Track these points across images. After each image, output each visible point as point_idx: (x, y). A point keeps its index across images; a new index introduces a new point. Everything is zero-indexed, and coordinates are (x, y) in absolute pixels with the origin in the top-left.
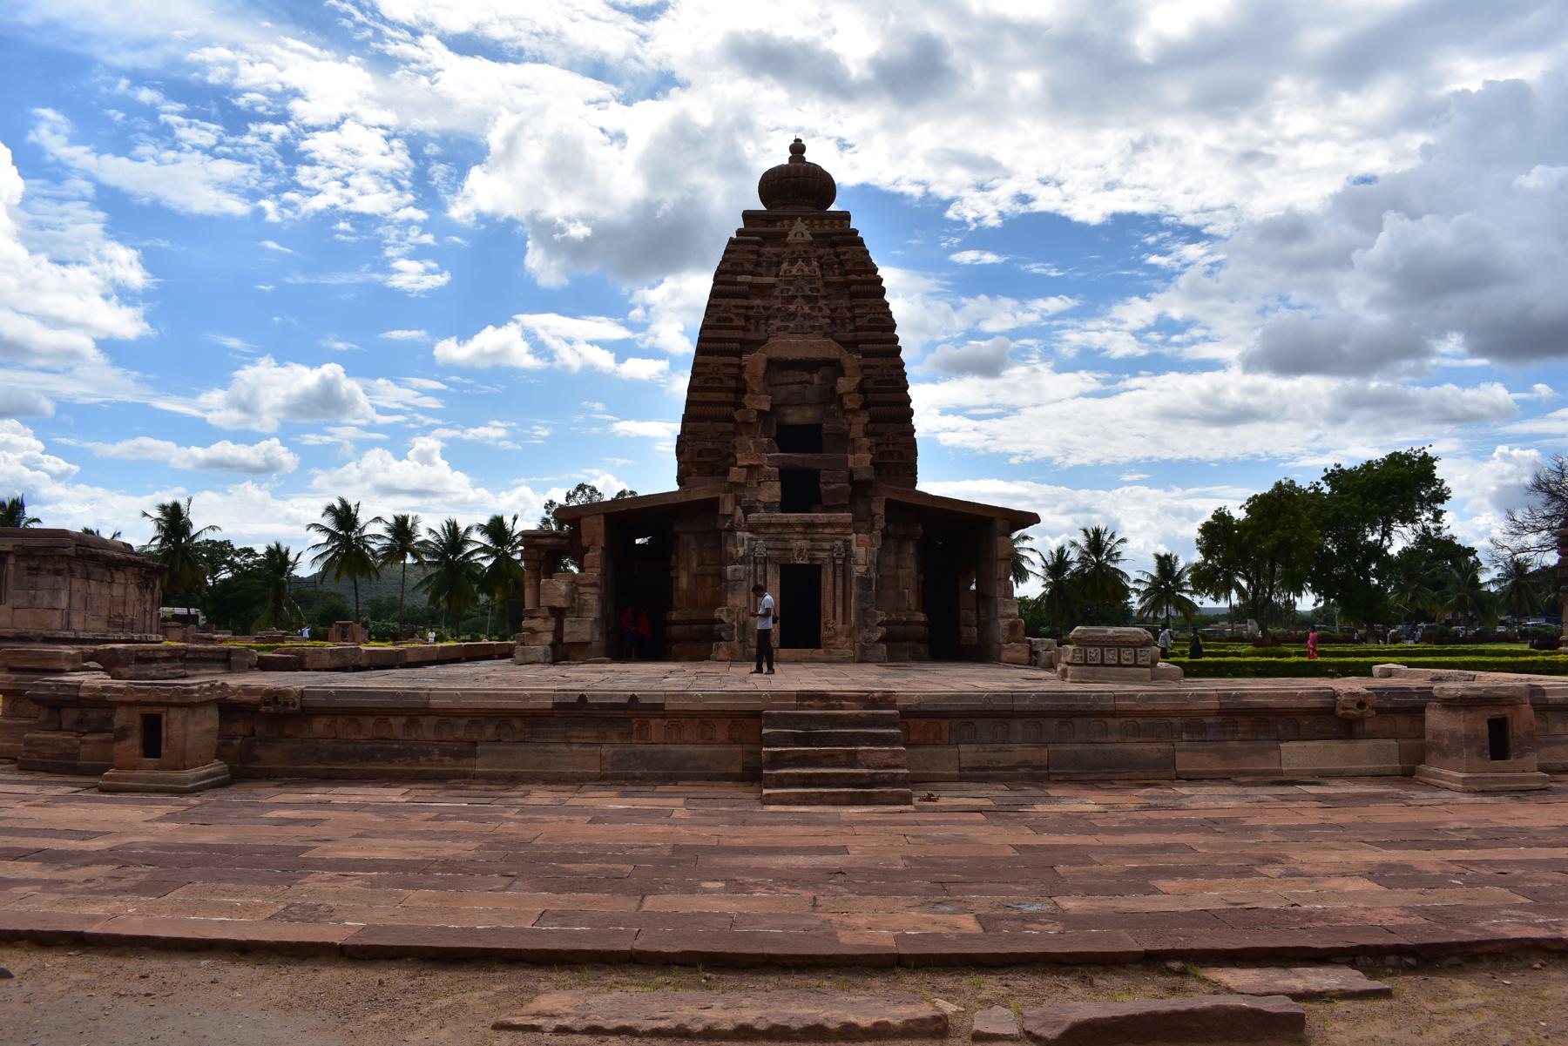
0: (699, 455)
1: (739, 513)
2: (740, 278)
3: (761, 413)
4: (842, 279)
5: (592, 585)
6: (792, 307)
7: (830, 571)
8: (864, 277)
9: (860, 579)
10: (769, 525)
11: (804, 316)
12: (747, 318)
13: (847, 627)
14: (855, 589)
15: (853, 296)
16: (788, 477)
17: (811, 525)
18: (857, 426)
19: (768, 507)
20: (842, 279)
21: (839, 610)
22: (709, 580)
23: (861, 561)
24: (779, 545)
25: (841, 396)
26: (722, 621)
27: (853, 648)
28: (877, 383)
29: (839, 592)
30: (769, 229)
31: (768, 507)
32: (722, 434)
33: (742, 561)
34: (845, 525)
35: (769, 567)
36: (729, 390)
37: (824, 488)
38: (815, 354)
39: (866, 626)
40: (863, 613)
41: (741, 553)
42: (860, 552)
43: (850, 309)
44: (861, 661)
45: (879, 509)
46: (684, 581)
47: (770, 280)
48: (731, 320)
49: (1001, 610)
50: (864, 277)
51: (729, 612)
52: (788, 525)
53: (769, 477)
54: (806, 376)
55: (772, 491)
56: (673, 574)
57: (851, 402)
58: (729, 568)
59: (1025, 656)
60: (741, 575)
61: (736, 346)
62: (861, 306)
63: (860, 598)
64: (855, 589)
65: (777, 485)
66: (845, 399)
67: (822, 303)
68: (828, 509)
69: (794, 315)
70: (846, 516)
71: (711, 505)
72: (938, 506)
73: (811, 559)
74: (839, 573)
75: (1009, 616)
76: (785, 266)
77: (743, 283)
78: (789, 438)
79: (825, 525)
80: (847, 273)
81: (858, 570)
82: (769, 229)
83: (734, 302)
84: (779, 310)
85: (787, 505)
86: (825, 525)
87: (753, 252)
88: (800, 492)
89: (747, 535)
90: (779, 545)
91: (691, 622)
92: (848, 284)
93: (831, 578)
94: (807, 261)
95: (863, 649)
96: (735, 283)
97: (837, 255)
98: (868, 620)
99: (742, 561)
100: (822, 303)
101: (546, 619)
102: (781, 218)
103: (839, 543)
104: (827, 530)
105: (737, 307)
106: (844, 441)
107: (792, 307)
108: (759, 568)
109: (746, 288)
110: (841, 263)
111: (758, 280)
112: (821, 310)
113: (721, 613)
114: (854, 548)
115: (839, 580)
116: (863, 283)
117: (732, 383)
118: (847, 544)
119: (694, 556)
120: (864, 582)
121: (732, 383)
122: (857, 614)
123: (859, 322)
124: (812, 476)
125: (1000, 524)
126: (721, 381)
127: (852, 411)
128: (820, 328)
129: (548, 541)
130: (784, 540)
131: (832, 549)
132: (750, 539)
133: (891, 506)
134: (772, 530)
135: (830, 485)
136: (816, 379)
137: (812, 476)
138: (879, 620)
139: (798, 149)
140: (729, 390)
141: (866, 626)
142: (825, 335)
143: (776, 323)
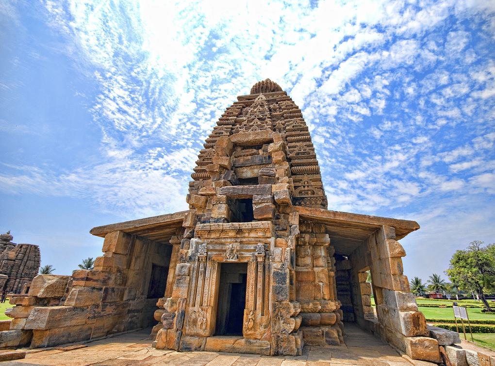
3: (222, 167)
4: (280, 113)
9: (276, 274)
10: (210, 232)
11: (258, 126)
13: (265, 318)
16: (229, 201)
17: (240, 231)
18: (280, 170)
23: (277, 259)
24: (218, 247)
28: (298, 154)
29: (260, 286)
31: (217, 220)
34: (265, 230)
35: (209, 265)
37: (255, 207)
41: (190, 254)
42: (276, 252)
43: (283, 125)
45: (294, 221)
53: (219, 201)
54: (255, 151)
55: (221, 211)
57: (278, 157)
63: (278, 291)
66: (273, 155)
74: (260, 269)
79: (250, 230)
81: (275, 266)
84: (245, 125)
85: (227, 220)
86: (250, 230)
88: (241, 210)
90: (218, 247)
93: (254, 275)
98: (284, 312)
103: (260, 244)
104: (253, 235)
106: (272, 179)
107: (251, 124)
112: (267, 123)
114: (272, 248)
115: (260, 274)
120: (280, 277)
122: (274, 306)
123: (287, 128)
131: (254, 250)
133: (303, 220)
134: (213, 236)
137: (248, 202)
138: (293, 311)
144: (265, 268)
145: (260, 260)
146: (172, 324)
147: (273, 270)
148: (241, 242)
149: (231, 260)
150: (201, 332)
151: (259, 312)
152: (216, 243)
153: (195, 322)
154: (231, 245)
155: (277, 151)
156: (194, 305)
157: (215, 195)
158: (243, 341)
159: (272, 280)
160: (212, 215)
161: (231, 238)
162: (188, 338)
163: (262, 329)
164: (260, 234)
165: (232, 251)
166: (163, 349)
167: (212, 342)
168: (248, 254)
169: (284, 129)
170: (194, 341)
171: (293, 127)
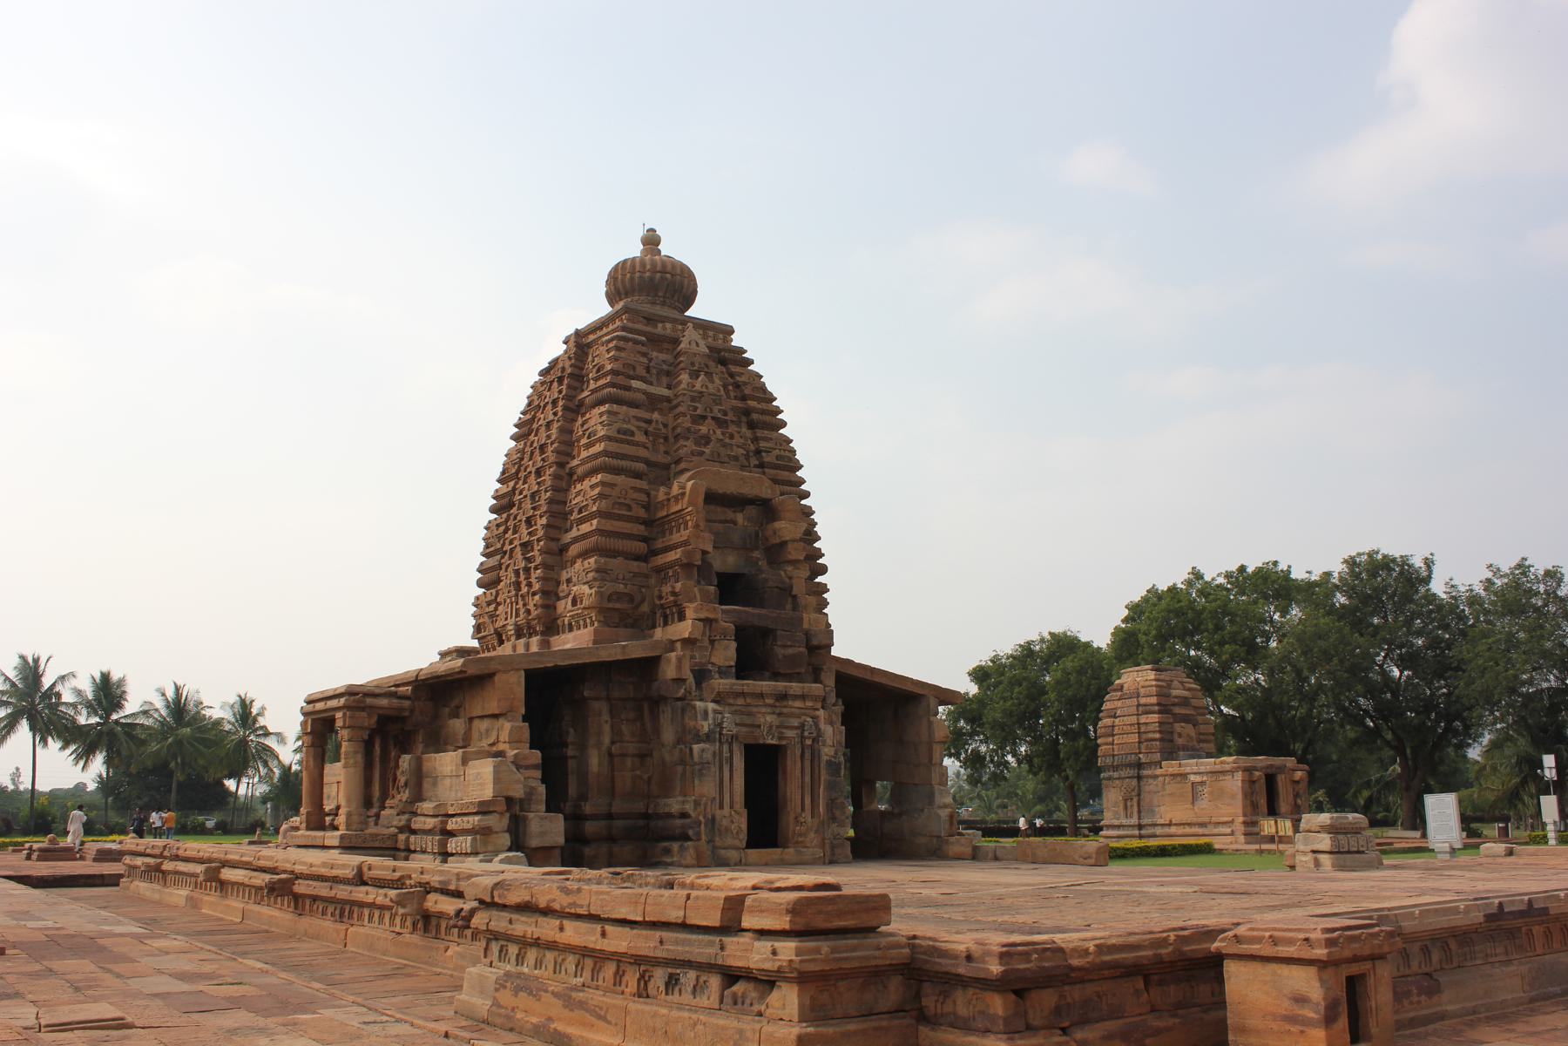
0: (609, 600)
1: (691, 680)
2: (635, 384)
4: (739, 404)
5: (535, 767)
6: (704, 429)
7: (798, 752)
8: (763, 406)
9: (829, 763)
12: (646, 433)
14: (824, 776)
15: (752, 426)
17: (783, 697)
19: (723, 672)
20: (739, 404)
21: (808, 801)
22: (629, 762)
23: (829, 742)
24: (748, 720)
25: (784, 544)
26: (684, 815)
27: (823, 846)
29: (808, 779)
30: (649, 329)
32: (635, 575)
33: (708, 738)
34: (815, 698)
35: (735, 747)
36: (637, 520)
37: (780, 652)
38: (748, 490)
39: (833, 819)
40: (832, 804)
41: (706, 729)
44: (832, 862)
46: (595, 762)
47: (666, 392)
48: (633, 434)
49: (939, 800)
50: (763, 406)
51: (697, 804)
52: (761, 696)
53: (725, 636)
54: (730, 514)
55: (727, 653)
56: (570, 752)
58: (696, 747)
59: (969, 850)
60: (708, 756)
61: (641, 466)
62: (768, 439)
63: (831, 787)
64: (824, 776)
65: (734, 645)
67: (732, 429)
68: (776, 676)
69: (706, 440)
70: (816, 688)
71: (647, 667)
72: (877, 679)
73: (780, 738)
75: (946, 806)
76: (685, 377)
77: (638, 390)
78: (730, 588)
79: (796, 697)
80: (744, 398)
81: (827, 752)
82: (649, 329)
83: (633, 412)
84: (688, 429)
86: (796, 697)
87: (644, 355)
89: (711, 706)
91: (610, 816)
92: (747, 412)
94: (709, 375)
95: (833, 847)
96: (628, 388)
97: (732, 375)
98: (837, 813)
99: (708, 738)
100: (732, 429)
101: (502, 814)
102: (663, 320)
104: (798, 704)
105: (638, 419)
107: (704, 429)
108: (726, 748)
109: (640, 397)
110: (737, 386)
111: (652, 389)
112: (732, 437)
113: (674, 805)
114: (822, 726)
115: (807, 764)
116: (763, 412)
117: (642, 513)
118: (815, 718)
119: (607, 728)
120: (833, 767)
121: (642, 513)
123: (767, 458)
124: (766, 633)
125: (933, 701)
126: (629, 508)
127: (794, 562)
128: (736, 458)
129: (384, 702)
130: (750, 714)
131: (802, 727)
132: (715, 711)
134: (740, 701)
135: (785, 649)
136: (740, 518)
139: (651, 241)
140: (637, 520)
141: (833, 819)
142: (743, 467)
143: (689, 446)
144: (815, 756)
145: (809, 742)
146: (698, 834)
147: (825, 758)
148: (780, 714)
149: (770, 741)
150: (737, 843)
151: (807, 814)
152: (743, 713)
153: (727, 830)
154: (769, 718)
155: (794, 541)
156: (721, 807)
157: (716, 620)
158: (791, 850)
159: (823, 772)
160: (713, 660)
161: (766, 705)
162: (722, 852)
163: (812, 835)
164: (809, 704)
165: (771, 727)
166: (693, 866)
167: (754, 853)
168: (790, 733)
169: (758, 452)
170: (733, 855)
171: (778, 457)
